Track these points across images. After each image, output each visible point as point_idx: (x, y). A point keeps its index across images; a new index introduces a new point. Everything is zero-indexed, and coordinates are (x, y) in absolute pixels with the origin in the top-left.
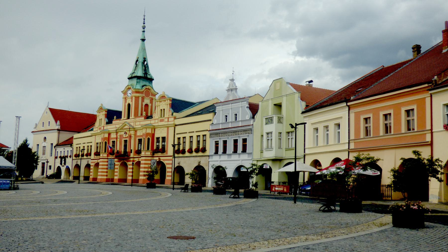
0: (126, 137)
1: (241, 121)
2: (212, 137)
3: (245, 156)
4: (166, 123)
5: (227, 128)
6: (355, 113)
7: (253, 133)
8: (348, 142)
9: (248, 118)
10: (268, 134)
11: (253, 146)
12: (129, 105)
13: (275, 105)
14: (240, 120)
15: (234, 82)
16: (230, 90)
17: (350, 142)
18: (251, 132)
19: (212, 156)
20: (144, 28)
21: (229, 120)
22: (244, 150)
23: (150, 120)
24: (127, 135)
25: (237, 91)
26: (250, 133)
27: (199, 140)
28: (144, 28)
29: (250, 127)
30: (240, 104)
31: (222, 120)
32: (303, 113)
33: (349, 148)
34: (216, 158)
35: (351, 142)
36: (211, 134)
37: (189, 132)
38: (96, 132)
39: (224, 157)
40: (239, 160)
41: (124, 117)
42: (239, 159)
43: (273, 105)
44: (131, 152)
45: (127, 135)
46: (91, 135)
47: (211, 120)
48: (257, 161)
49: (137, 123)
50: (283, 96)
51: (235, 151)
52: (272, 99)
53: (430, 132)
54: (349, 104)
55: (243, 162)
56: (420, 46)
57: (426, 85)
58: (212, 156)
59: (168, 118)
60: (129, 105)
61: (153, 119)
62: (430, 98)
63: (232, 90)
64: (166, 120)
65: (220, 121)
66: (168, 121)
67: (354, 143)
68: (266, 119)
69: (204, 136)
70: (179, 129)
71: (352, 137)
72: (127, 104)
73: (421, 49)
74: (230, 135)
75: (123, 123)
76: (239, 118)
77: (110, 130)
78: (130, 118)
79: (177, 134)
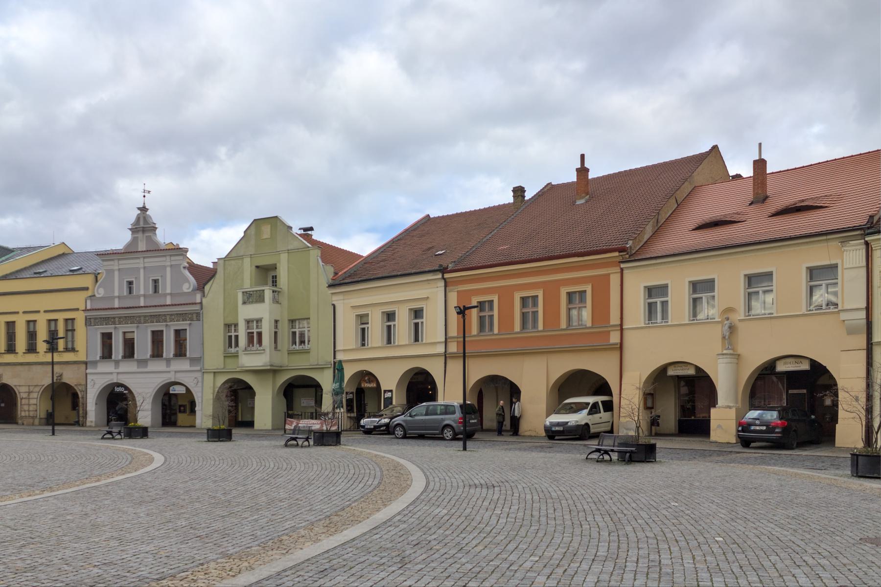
1: (171, 294)
2: (92, 324)
3: (182, 365)
5: (133, 307)
6: (458, 291)
7: (201, 319)
8: (443, 340)
9: (188, 289)
10: (248, 322)
11: (203, 344)
13: (257, 267)
14: (168, 291)
15: (148, 213)
16: (139, 229)
17: (449, 340)
18: (197, 316)
19: (95, 363)
21: (140, 290)
22: (180, 352)
25: (156, 234)
26: (195, 319)
27: (53, 328)
29: (197, 307)
30: (167, 261)
31: (118, 288)
32: (330, 286)
33: (446, 351)
34: (106, 367)
35: (450, 342)
36: (90, 319)
37: (24, 312)
39: (128, 366)
40: (169, 372)
42: (168, 369)
43: (254, 267)
47: (87, 289)
48: (214, 373)
50: (280, 252)
51: (157, 353)
52: (252, 256)
53: (619, 328)
54: (447, 276)
55: (178, 375)
56: (524, 188)
57: (617, 254)
62: (619, 275)
65: (113, 291)
67: (456, 343)
68: (243, 292)
69: (66, 320)
73: (526, 194)
74: (142, 322)
76: (167, 287)
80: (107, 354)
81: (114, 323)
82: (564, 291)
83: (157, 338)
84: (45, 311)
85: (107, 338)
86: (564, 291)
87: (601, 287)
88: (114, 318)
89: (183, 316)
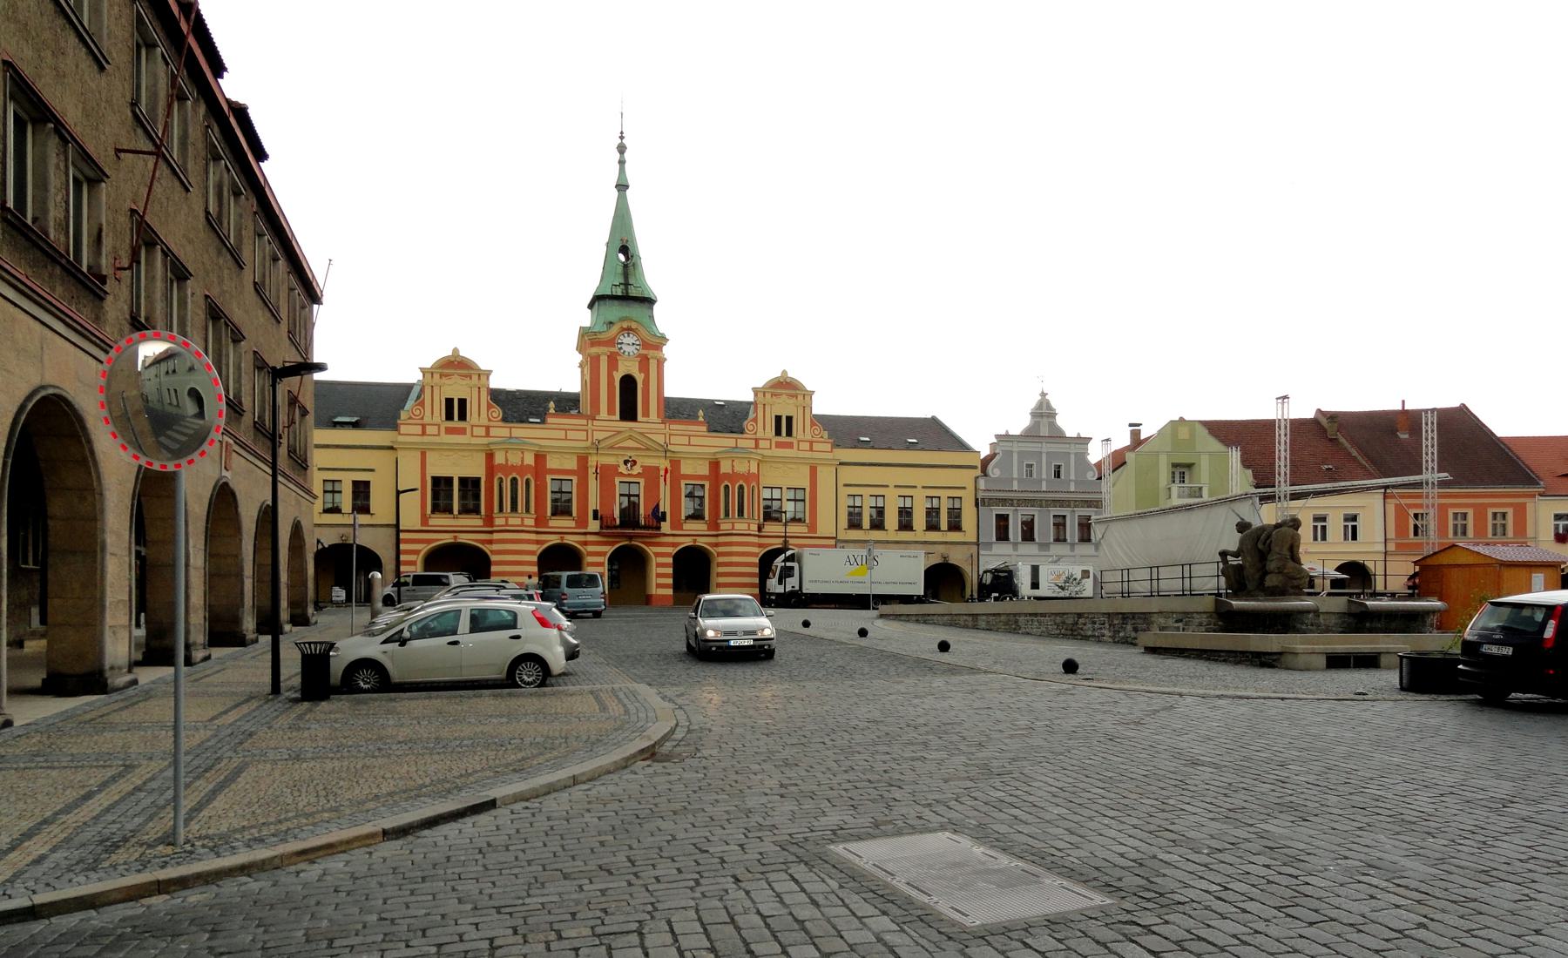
0: (635, 472)
4: (808, 455)
12: (628, 383)
19: (989, 545)
20: (622, 149)
23: (736, 439)
24: (637, 470)
28: (622, 149)
30: (1073, 449)
38: (437, 439)
41: (611, 411)
42: (1072, 554)
44: (664, 520)
45: (637, 470)
46: (390, 444)
49: (674, 440)
58: (991, 544)
59: (811, 443)
60: (628, 383)
61: (745, 436)
63: (1041, 415)
64: (806, 447)
66: (811, 450)
70: (848, 475)
71: (1391, 534)
72: (618, 377)
75: (619, 432)
77: (542, 443)
78: (640, 417)
79: (846, 485)
80: (1003, 535)
81: (1012, 505)
82: (1490, 512)
83: (1060, 524)
84: (923, 487)
85: (1002, 520)
86: (1490, 512)
87: (1521, 511)
88: (1012, 500)
89: (1088, 503)
